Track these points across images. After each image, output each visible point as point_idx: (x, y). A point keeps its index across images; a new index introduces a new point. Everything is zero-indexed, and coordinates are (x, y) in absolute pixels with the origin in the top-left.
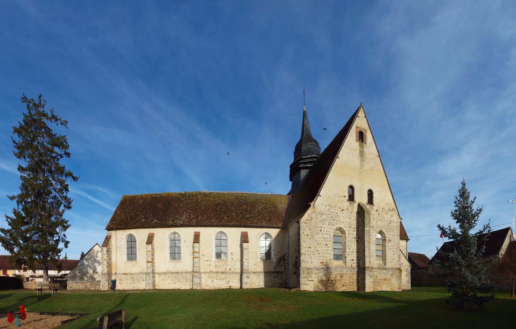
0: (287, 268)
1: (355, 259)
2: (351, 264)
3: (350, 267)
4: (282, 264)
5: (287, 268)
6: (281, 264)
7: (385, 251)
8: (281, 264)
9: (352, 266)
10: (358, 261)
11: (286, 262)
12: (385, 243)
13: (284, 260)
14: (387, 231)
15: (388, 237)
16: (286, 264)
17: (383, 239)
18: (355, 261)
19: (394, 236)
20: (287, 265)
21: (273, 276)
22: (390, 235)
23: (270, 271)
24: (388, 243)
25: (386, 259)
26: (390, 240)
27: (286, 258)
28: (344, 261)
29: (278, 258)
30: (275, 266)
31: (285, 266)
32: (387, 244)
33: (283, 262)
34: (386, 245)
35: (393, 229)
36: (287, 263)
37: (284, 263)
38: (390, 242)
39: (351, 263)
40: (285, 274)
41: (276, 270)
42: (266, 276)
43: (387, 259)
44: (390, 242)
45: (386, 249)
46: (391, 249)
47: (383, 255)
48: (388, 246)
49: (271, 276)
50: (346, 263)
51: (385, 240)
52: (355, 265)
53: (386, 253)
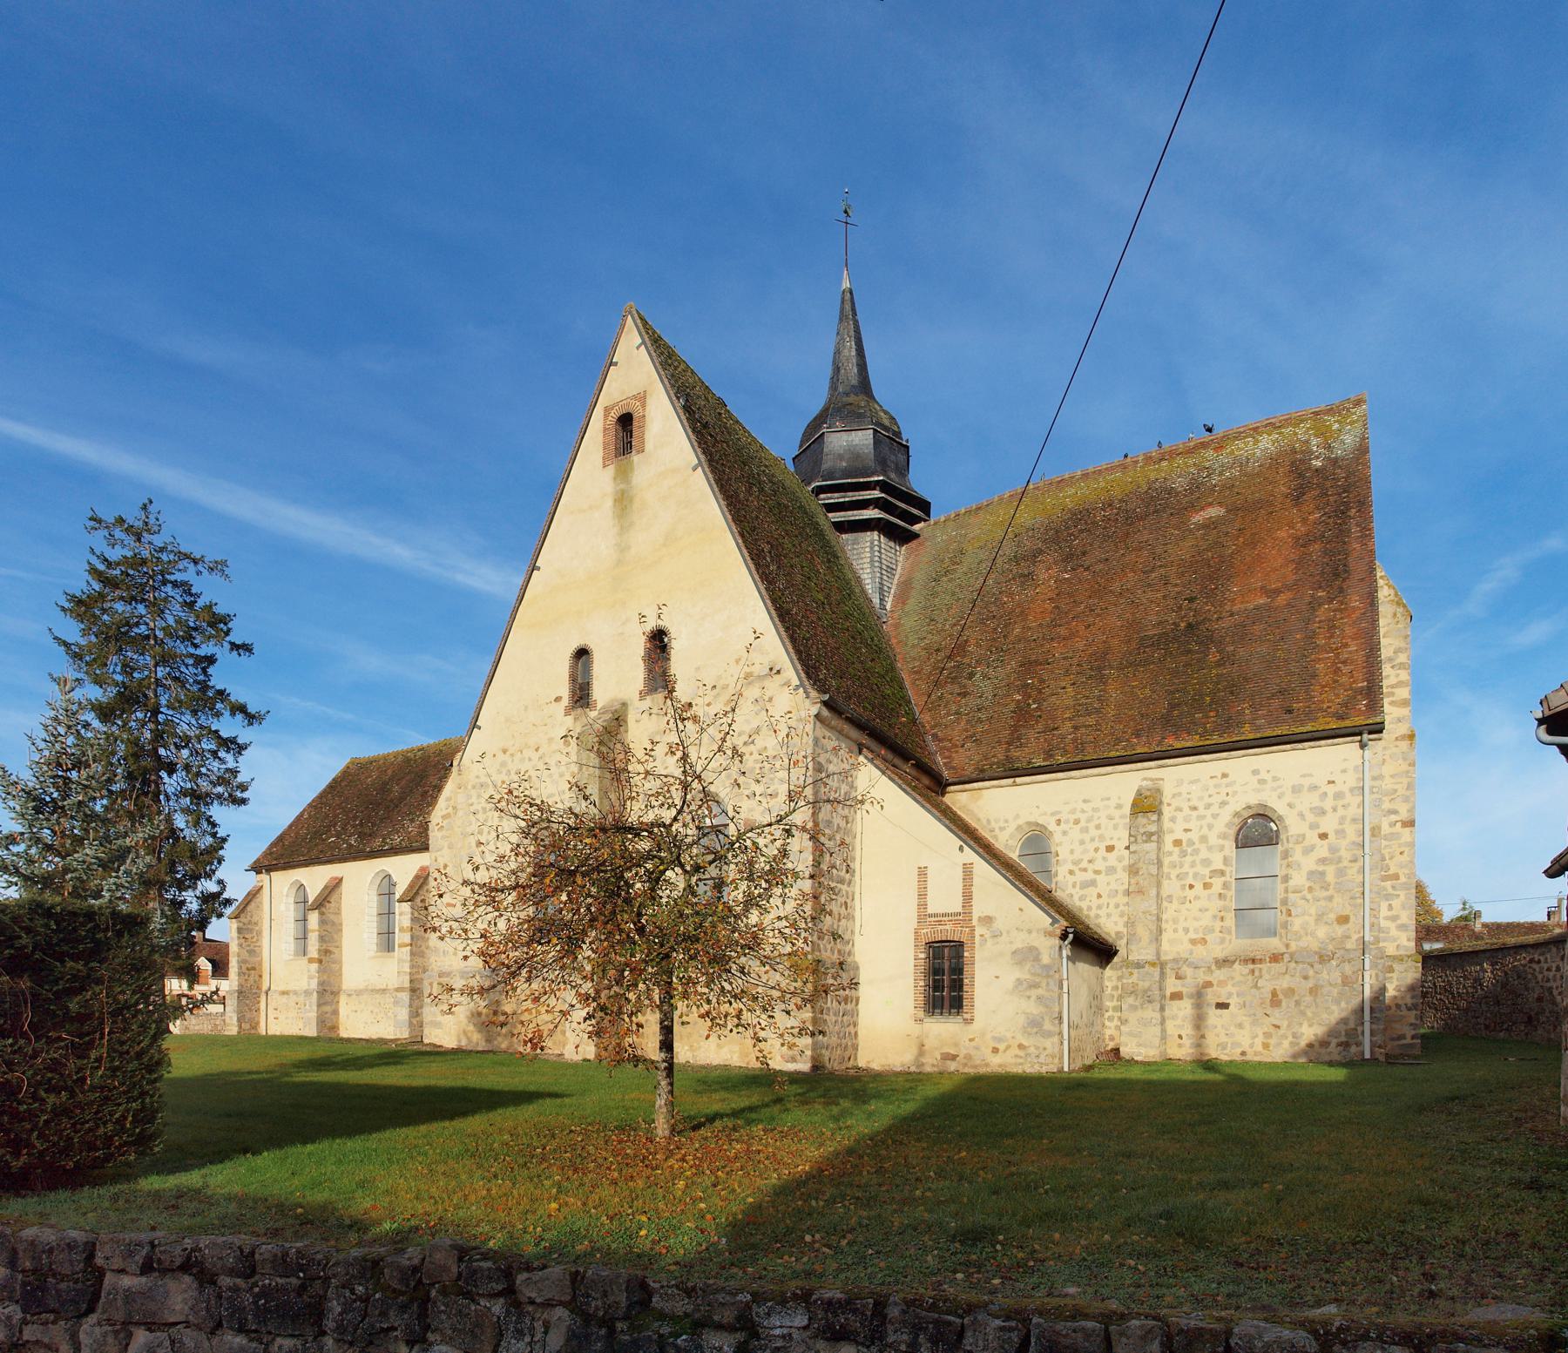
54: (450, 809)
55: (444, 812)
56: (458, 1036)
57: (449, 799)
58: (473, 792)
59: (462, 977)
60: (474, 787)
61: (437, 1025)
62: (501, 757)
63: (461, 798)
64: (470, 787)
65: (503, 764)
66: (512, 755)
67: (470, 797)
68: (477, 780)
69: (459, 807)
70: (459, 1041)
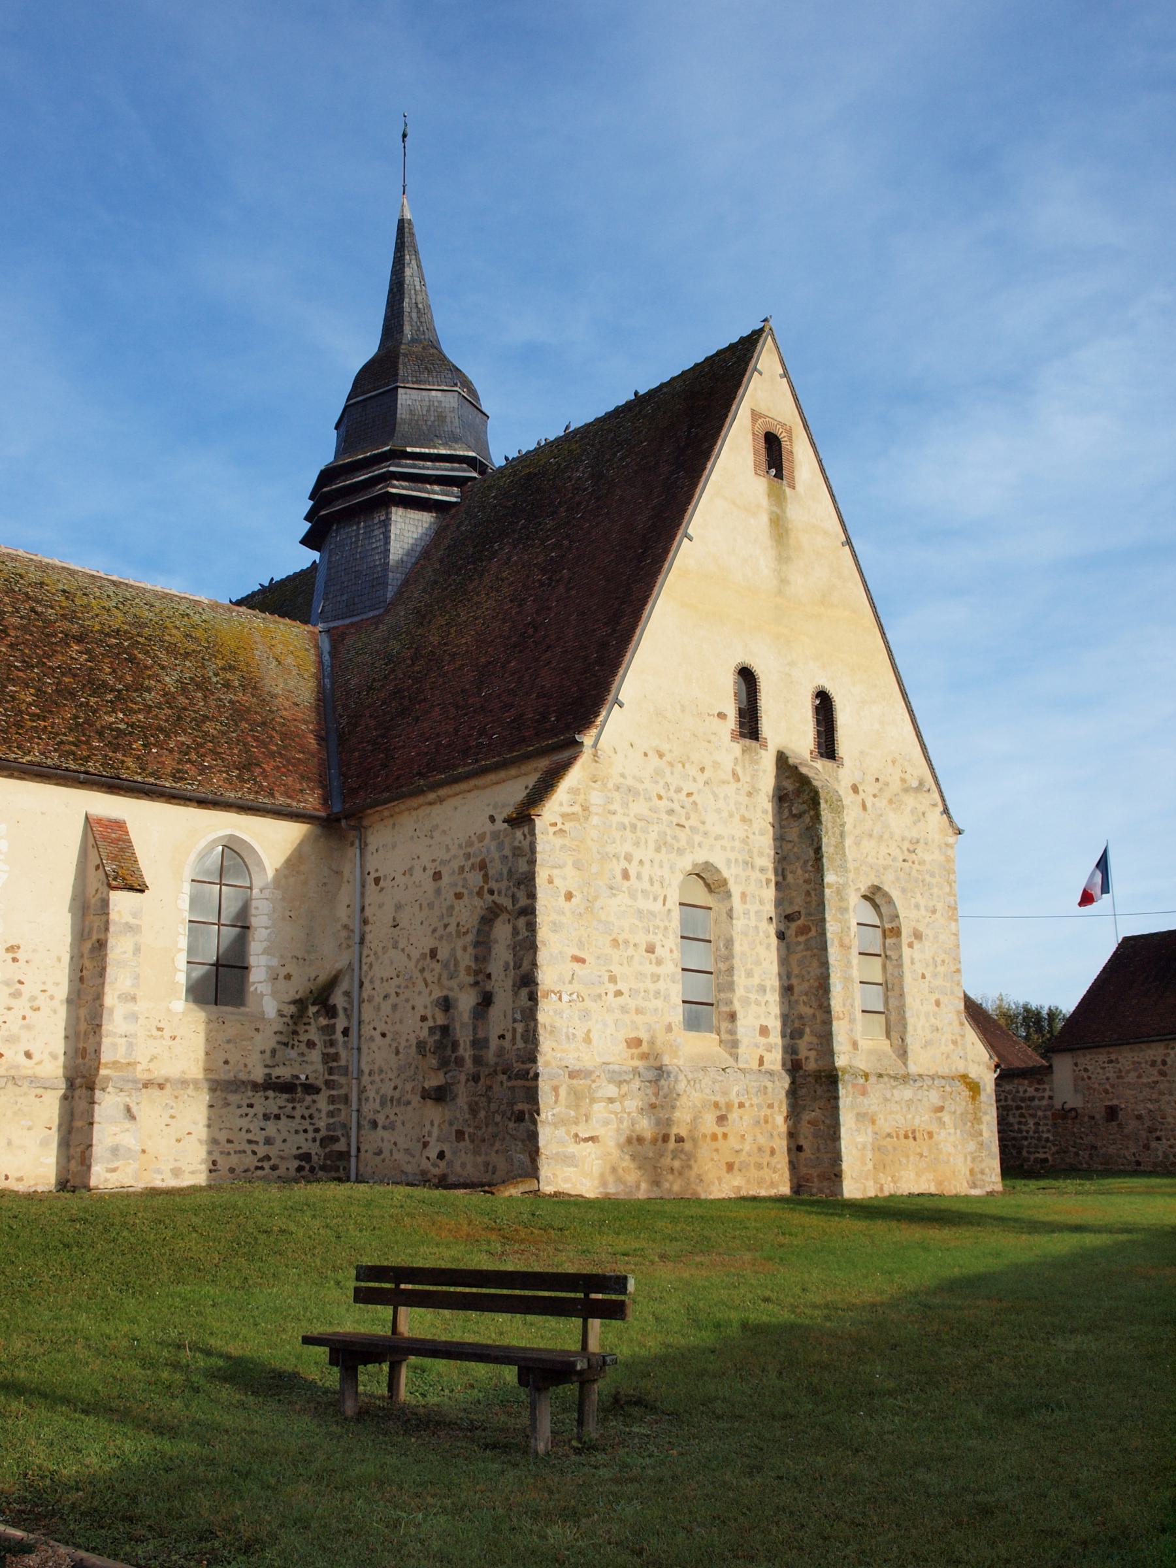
0: (343, 1063)
1: (775, 1025)
2: (760, 1051)
3: (755, 1065)
4: (314, 1034)
5: (343, 1063)
6: (304, 1038)
7: (897, 988)
8: (304, 1038)
9: (761, 1061)
10: (788, 1037)
11: (341, 1023)
12: (898, 947)
13: (331, 1012)
14: (904, 891)
15: (909, 916)
16: (339, 1036)
17: (888, 926)
18: (776, 1039)
19: (934, 912)
20: (345, 1042)
21: (259, 1109)
22: (917, 906)
23: (243, 1076)
24: (911, 945)
25: (905, 1026)
26: (918, 935)
27: (338, 1000)
28: (725, 1036)
29: (293, 995)
30: (272, 1043)
31: (332, 1051)
32: (906, 951)
33: (323, 1021)
34: (901, 956)
35: (928, 878)
36: (346, 1032)
37: (329, 1030)
38: (917, 945)
39: (757, 1046)
40: (332, 1100)
41: (277, 1072)
42: (224, 1111)
43: (910, 1028)
44: (917, 945)
45: (901, 977)
46: (923, 977)
47: (891, 1006)
48: (912, 963)
49: (251, 1111)
50: (735, 1044)
51: (896, 932)
52: (775, 1059)
53: (902, 995)
54: (577, 809)
55: (567, 809)
56: (602, 1175)
57: (574, 791)
58: (616, 795)
59: (611, 1081)
60: (618, 788)
61: (568, 1160)
62: (654, 760)
63: (596, 798)
64: (610, 785)
65: (658, 772)
66: (671, 764)
67: (610, 801)
68: (621, 780)
69: (593, 809)
70: (604, 1184)
